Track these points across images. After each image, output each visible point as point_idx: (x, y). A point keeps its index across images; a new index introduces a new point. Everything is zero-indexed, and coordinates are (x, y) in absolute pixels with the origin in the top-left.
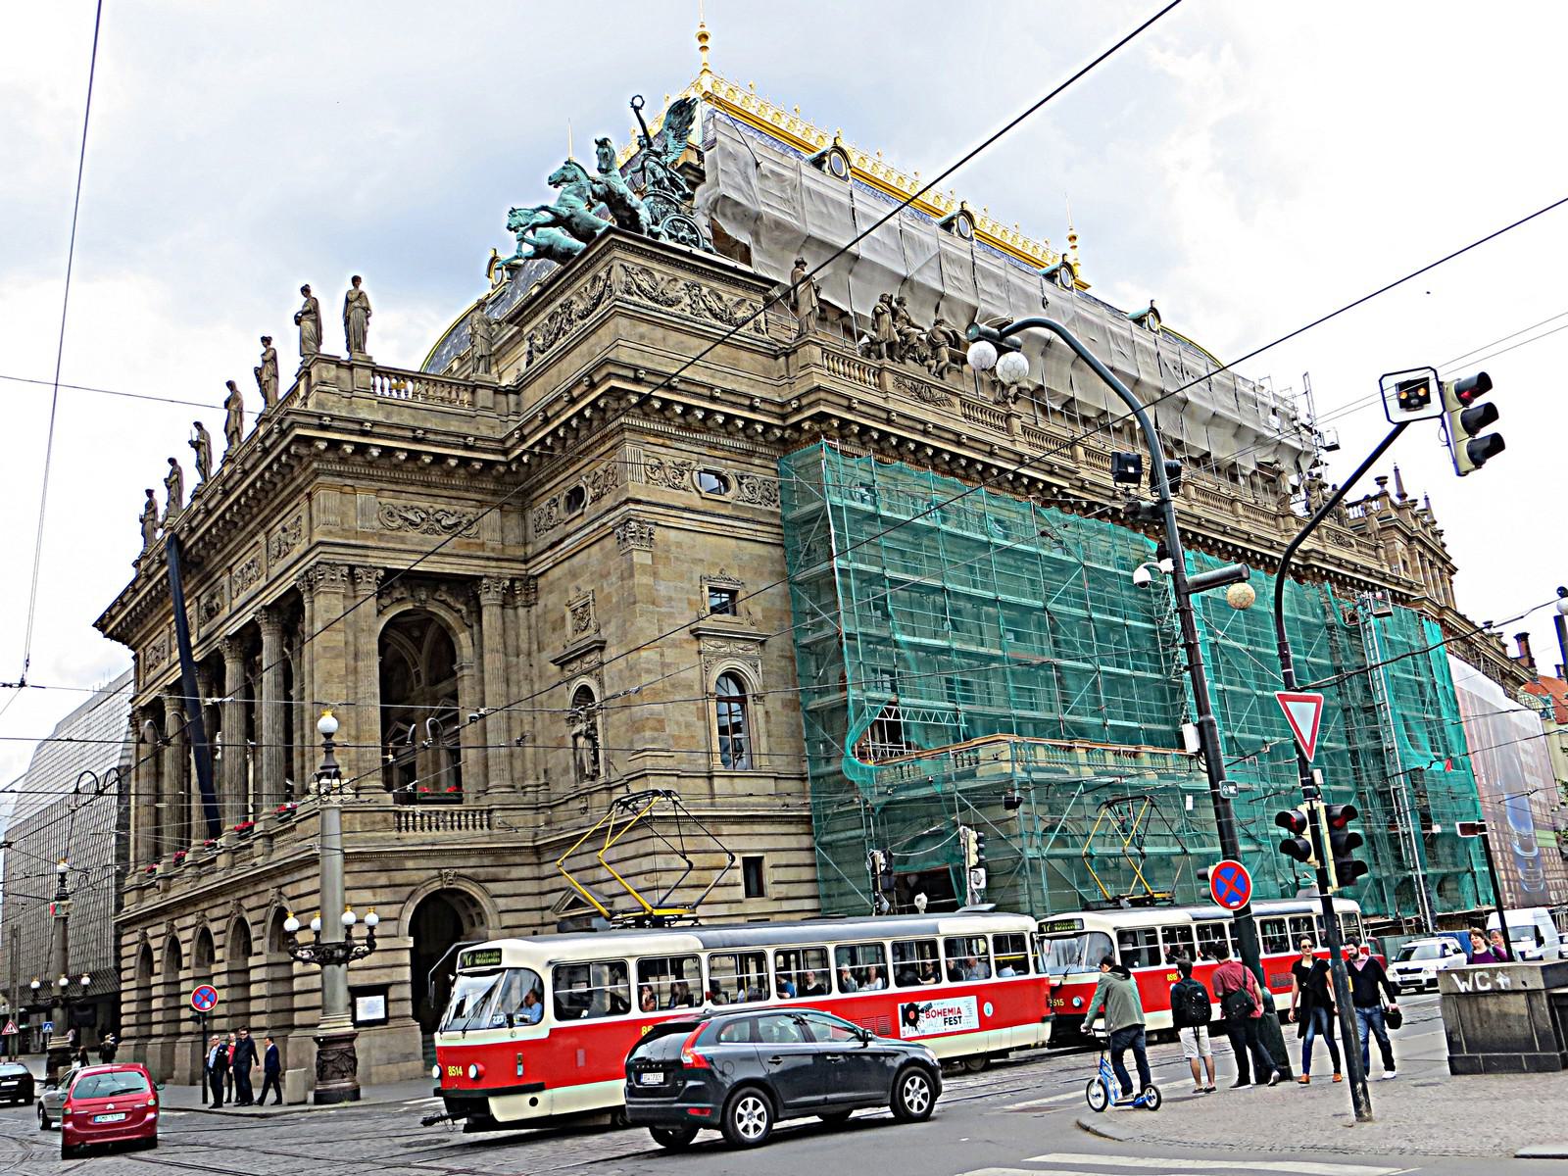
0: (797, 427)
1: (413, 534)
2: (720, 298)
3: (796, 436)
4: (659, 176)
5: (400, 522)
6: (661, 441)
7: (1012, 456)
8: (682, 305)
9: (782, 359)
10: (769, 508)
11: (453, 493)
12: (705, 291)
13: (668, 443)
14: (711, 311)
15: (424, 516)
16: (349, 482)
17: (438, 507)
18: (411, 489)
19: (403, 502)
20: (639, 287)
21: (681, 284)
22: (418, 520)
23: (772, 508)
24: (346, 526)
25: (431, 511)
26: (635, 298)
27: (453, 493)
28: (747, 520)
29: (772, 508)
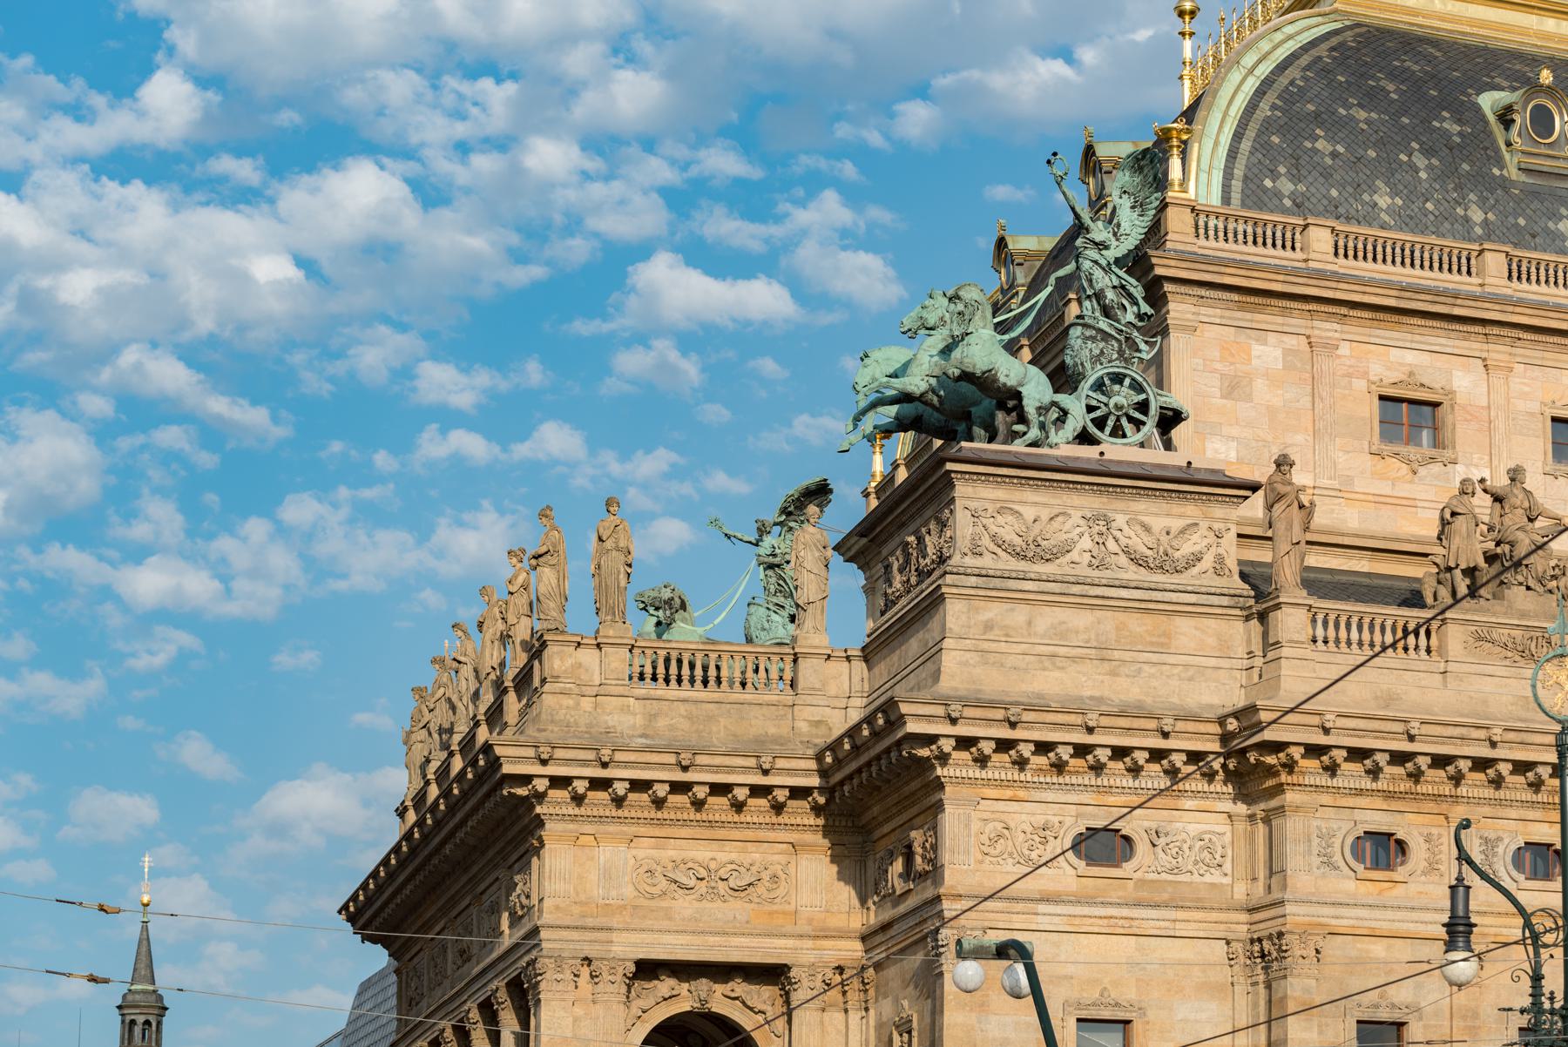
1: (684, 905)
2: (1147, 529)
4: (1098, 286)
5: (664, 883)
6: (1009, 793)
8: (1074, 555)
10: (1208, 878)
11: (750, 835)
12: (1120, 520)
13: (1022, 794)
14: (1126, 551)
15: (703, 873)
16: (588, 828)
17: (723, 857)
18: (685, 832)
19: (671, 853)
20: (994, 537)
21: (1076, 516)
22: (692, 882)
23: (1215, 877)
24: (583, 897)
25: (713, 866)
26: (986, 562)
27: (750, 835)
28: (1157, 906)
29: (1215, 877)
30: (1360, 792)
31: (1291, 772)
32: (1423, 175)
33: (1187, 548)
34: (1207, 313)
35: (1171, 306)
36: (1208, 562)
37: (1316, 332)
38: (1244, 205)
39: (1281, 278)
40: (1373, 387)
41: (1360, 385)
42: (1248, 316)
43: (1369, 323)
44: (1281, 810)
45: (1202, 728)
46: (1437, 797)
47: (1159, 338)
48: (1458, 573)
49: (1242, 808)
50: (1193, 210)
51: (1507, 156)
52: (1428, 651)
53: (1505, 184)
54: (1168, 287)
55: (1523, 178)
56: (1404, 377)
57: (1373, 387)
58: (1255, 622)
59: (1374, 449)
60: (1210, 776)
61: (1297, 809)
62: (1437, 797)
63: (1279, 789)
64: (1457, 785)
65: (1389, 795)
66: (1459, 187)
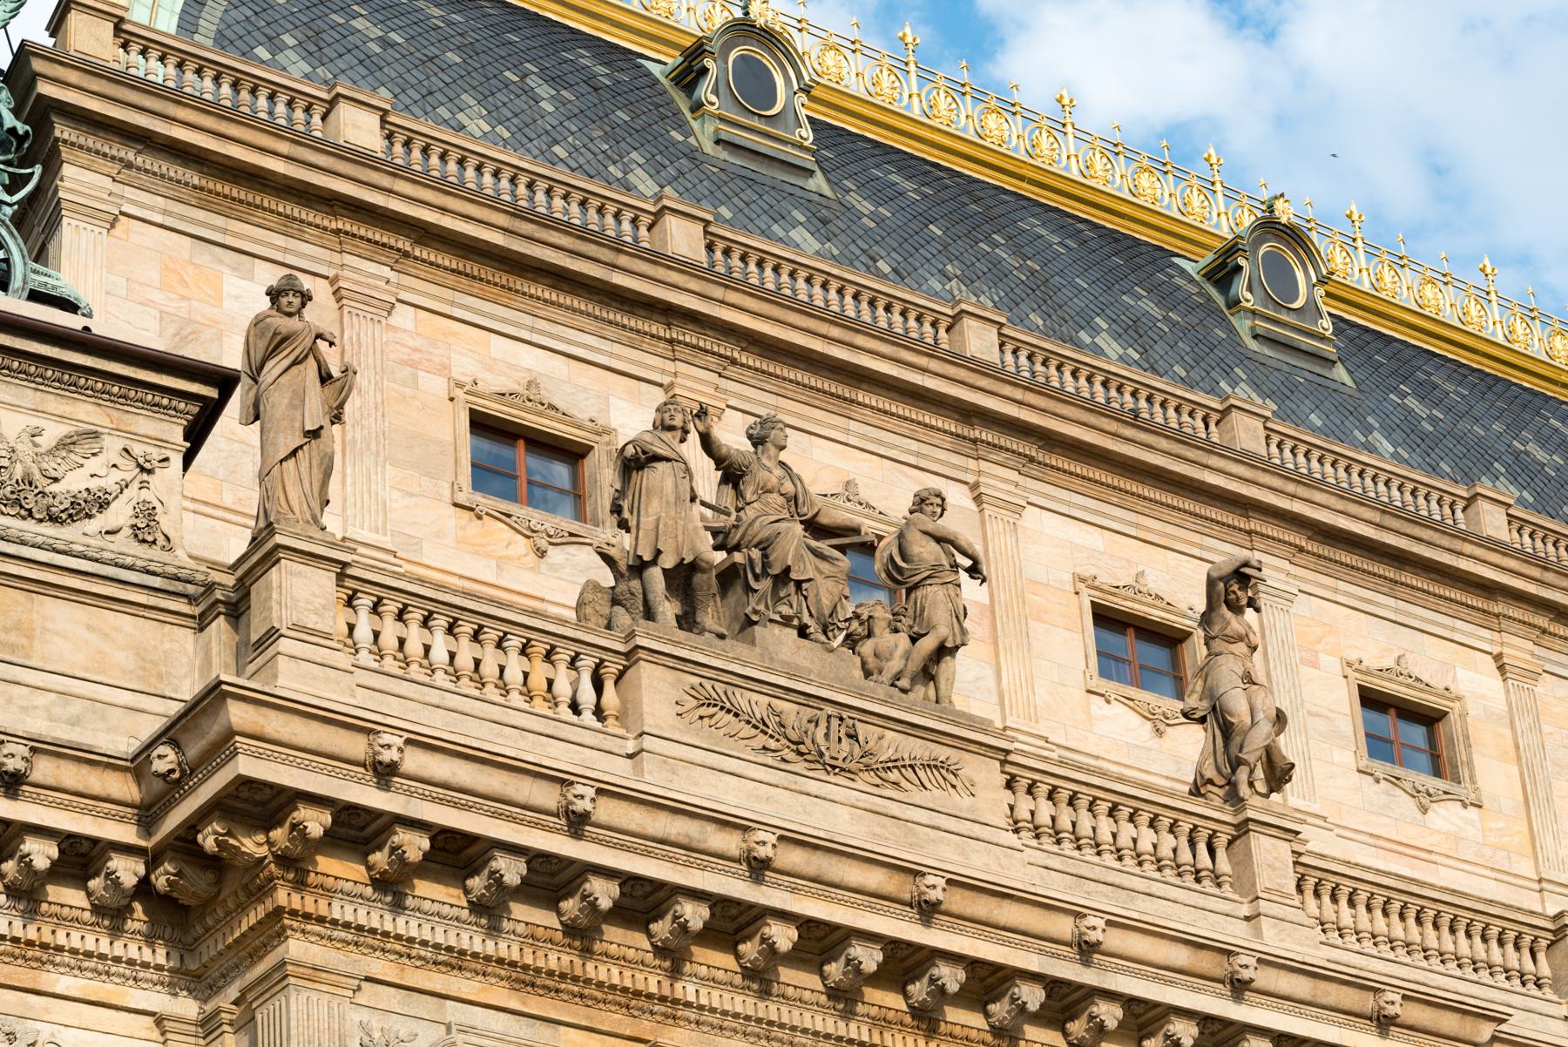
0: (184, 843)
3: (199, 883)
7: (1180, 956)
9: (220, 626)
30: (456, 961)
31: (300, 884)
32: (547, 107)
33: (75, 482)
34: (136, 199)
35: (67, 170)
36: (120, 514)
37: (346, 273)
38: (221, 40)
39: (284, 147)
40: (459, 393)
41: (436, 385)
42: (219, 221)
43: (451, 279)
44: (278, 977)
45: (96, 781)
46: (629, 999)
47: (38, 170)
48: (656, 576)
49: (187, 1007)
50: (118, 30)
51: (695, 125)
52: (599, 713)
53: (694, 155)
54: (62, 131)
55: (723, 154)
56: (514, 387)
57: (459, 393)
58: (220, 626)
59: (462, 498)
60: (111, 915)
61: (315, 973)
62: (629, 999)
63: (274, 927)
64: (675, 973)
65: (524, 978)
66: (611, 137)
